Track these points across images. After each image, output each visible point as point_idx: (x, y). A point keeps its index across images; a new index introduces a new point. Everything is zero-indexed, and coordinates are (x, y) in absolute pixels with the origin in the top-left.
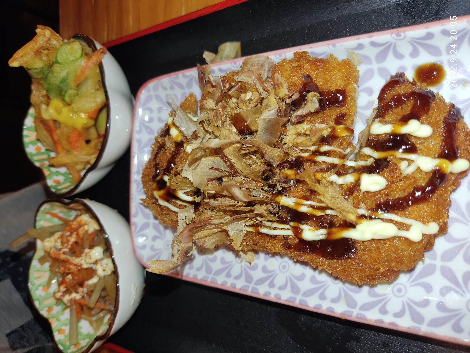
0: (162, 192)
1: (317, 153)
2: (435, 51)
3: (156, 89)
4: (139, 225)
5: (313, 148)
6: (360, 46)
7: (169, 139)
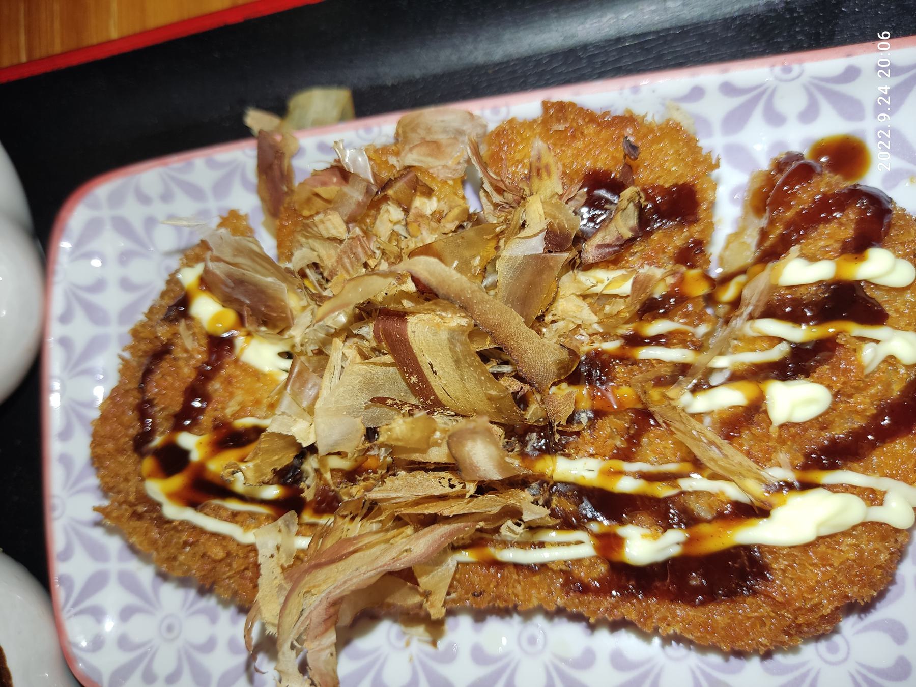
0: (177, 482)
1: (636, 340)
2: (850, 107)
3: (116, 199)
4: (79, 584)
5: (627, 330)
6: (697, 93)
7: (189, 327)
